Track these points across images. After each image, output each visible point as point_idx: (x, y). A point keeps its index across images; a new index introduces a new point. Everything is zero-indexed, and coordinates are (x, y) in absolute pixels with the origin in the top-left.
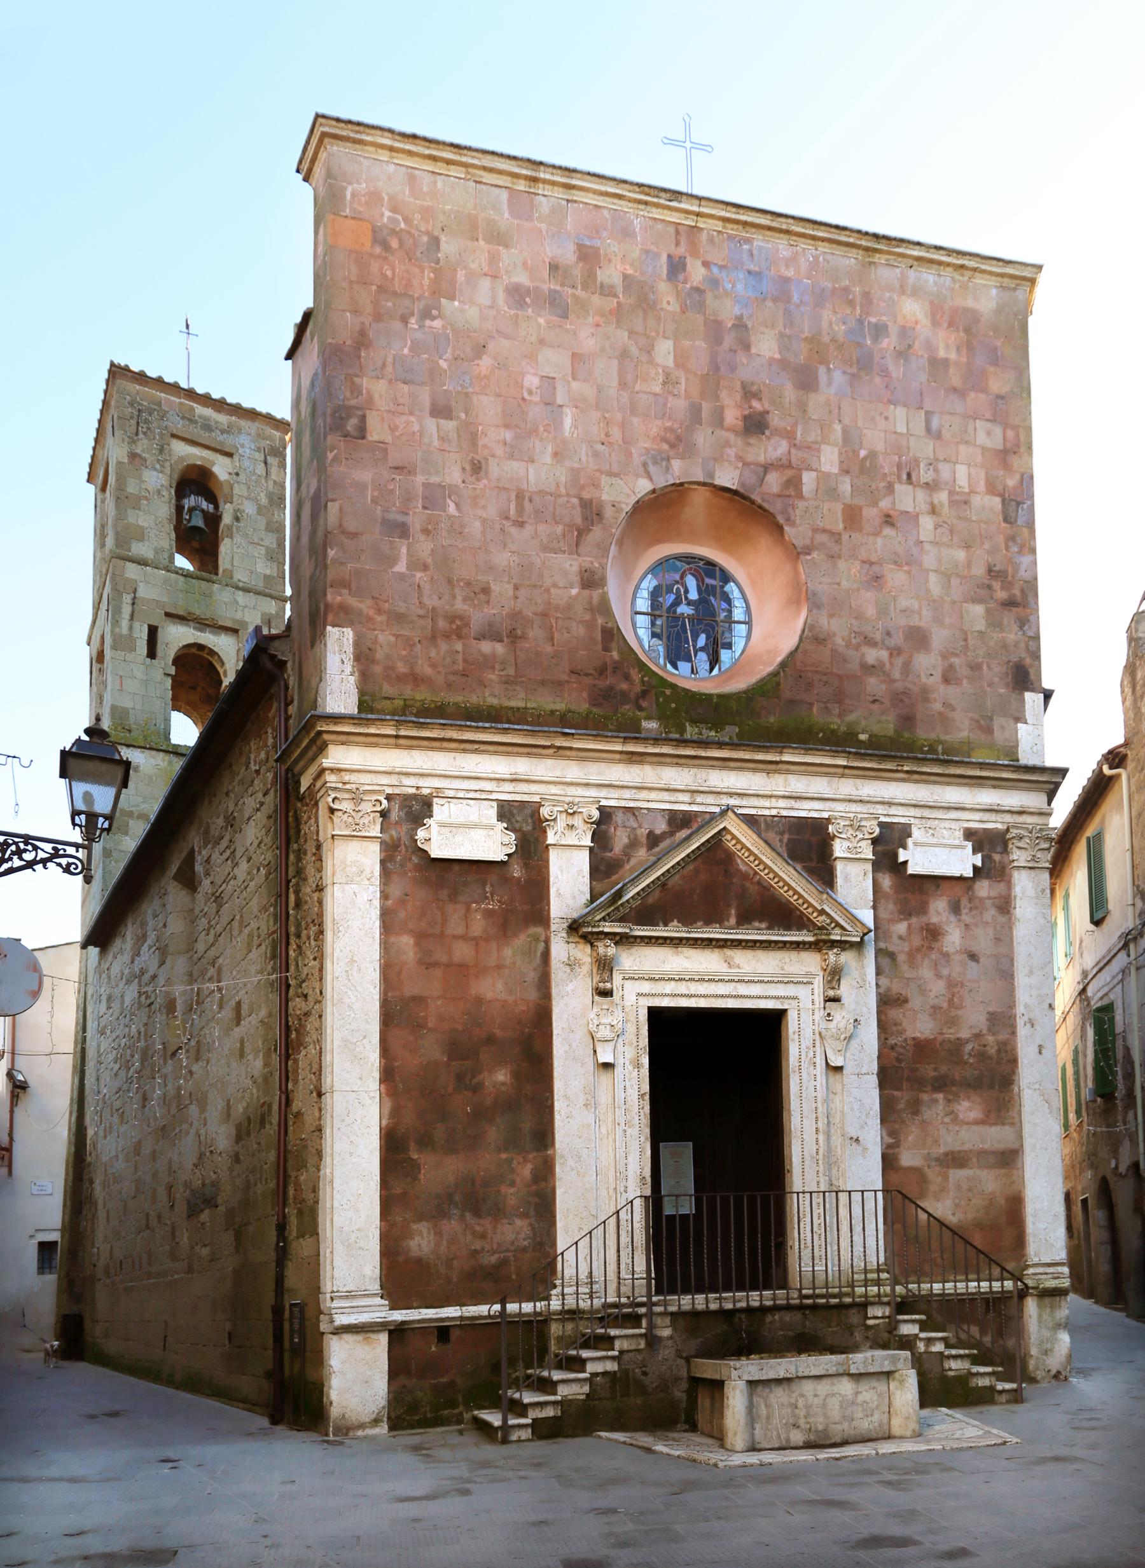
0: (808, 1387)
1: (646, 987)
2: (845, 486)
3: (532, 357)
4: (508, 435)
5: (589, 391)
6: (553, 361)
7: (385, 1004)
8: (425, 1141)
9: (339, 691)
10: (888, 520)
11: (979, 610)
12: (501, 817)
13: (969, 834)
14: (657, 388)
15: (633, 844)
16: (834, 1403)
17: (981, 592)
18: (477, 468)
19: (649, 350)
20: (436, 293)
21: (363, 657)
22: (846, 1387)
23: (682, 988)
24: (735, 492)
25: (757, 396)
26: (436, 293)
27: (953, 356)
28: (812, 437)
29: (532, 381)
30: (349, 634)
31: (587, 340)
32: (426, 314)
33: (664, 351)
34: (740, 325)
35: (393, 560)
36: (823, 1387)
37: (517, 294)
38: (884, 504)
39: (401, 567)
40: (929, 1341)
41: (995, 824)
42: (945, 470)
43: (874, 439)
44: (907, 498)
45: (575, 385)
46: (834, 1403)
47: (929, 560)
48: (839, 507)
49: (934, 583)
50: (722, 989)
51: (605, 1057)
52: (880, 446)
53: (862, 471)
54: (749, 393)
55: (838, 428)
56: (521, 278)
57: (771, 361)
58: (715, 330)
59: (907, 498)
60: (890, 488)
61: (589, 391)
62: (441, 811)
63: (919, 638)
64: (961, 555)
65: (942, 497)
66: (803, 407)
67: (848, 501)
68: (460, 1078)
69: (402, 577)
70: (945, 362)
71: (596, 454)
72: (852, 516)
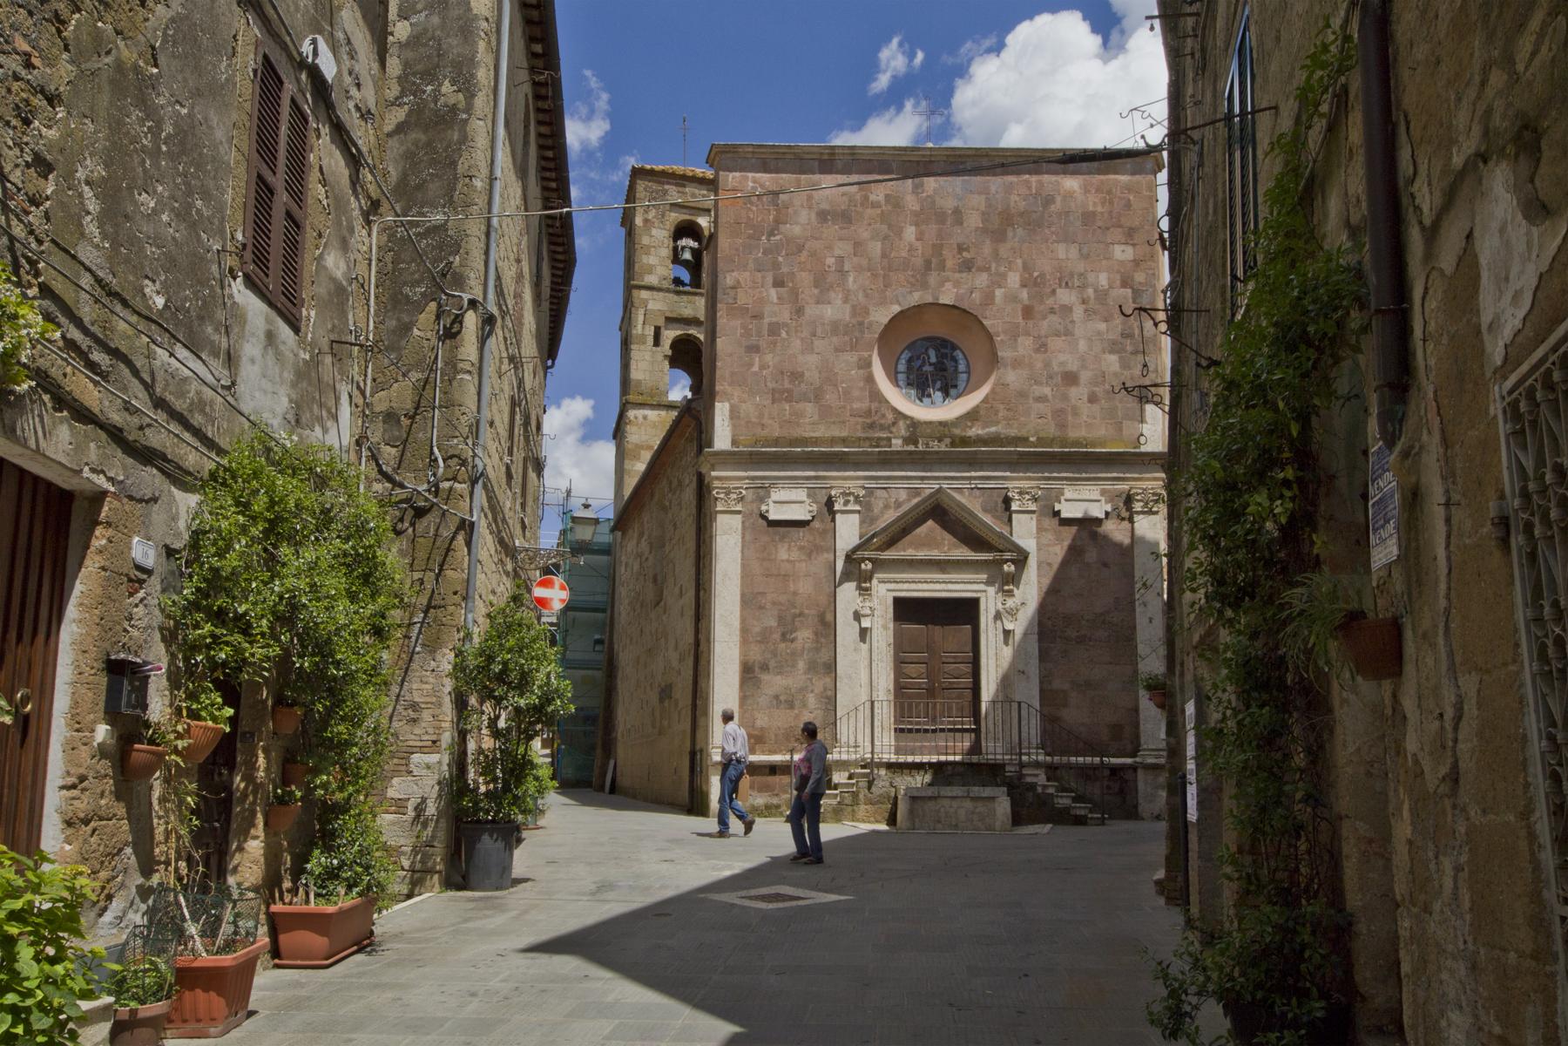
0: (946, 802)
1: (892, 586)
2: (1024, 294)
3: (830, 248)
4: (816, 291)
5: (865, 262)
6: (842, 248)
7: (743, 595)
8: (765, 667)
9: (722, 439)
10: (1052, 311)
11: (1113, 358)
12: (809, 496)
13: (1103, 493)
14: (904, 254)
15: (887, 507)
16: (962, 812)
17: (1114, 347)
18: (799, 311)
19: (899, 233)
20: (777, 222)
21: (734, 414)
22: (968, 804)
23: (913, 586)
24: (954, 307)
25: (967, 250)
26: (777, 222)
27: (1099, 209)
28: (1002, 269)
29: (830, 261)
30: (727, 405)
31: (865, 234)
32: (771, 234)
33: (910, 232)
34: (957, 212)
35: (752, 365)
36: (955, 804)
37: (823, 216)
38: (1050, 302)
39: (756, 368)
40: (1045, 787)
41: (1124, 486)
42: (1091, 277)
43: (1044, 265)
44: (1065, 296)
45: (855, 259)
46: (962, 812)
47: (1079, 331)
48: (1019, 307)
49: (1082, 345)
50: (938, 587)
51: (866, 623)
52: (1048, 269)
53: (1036, 284)
54: (961, 249)
55: (1019, 261)
56: (825, 206)
57: (977, 229)
58: (941, 217)
59: (1065, 296)
60: (1054, 292)
61: (865, 262)
62: (776, 495)
63: (1071, 378)
64: (1103, 326)
65: (1090, 291)
66: (996, 254)
67: (1027, 302)
68: (783, 635)
69: (755, 374)
70: (1094, 214)
71: (867, 296)
72: (1028, 312)
